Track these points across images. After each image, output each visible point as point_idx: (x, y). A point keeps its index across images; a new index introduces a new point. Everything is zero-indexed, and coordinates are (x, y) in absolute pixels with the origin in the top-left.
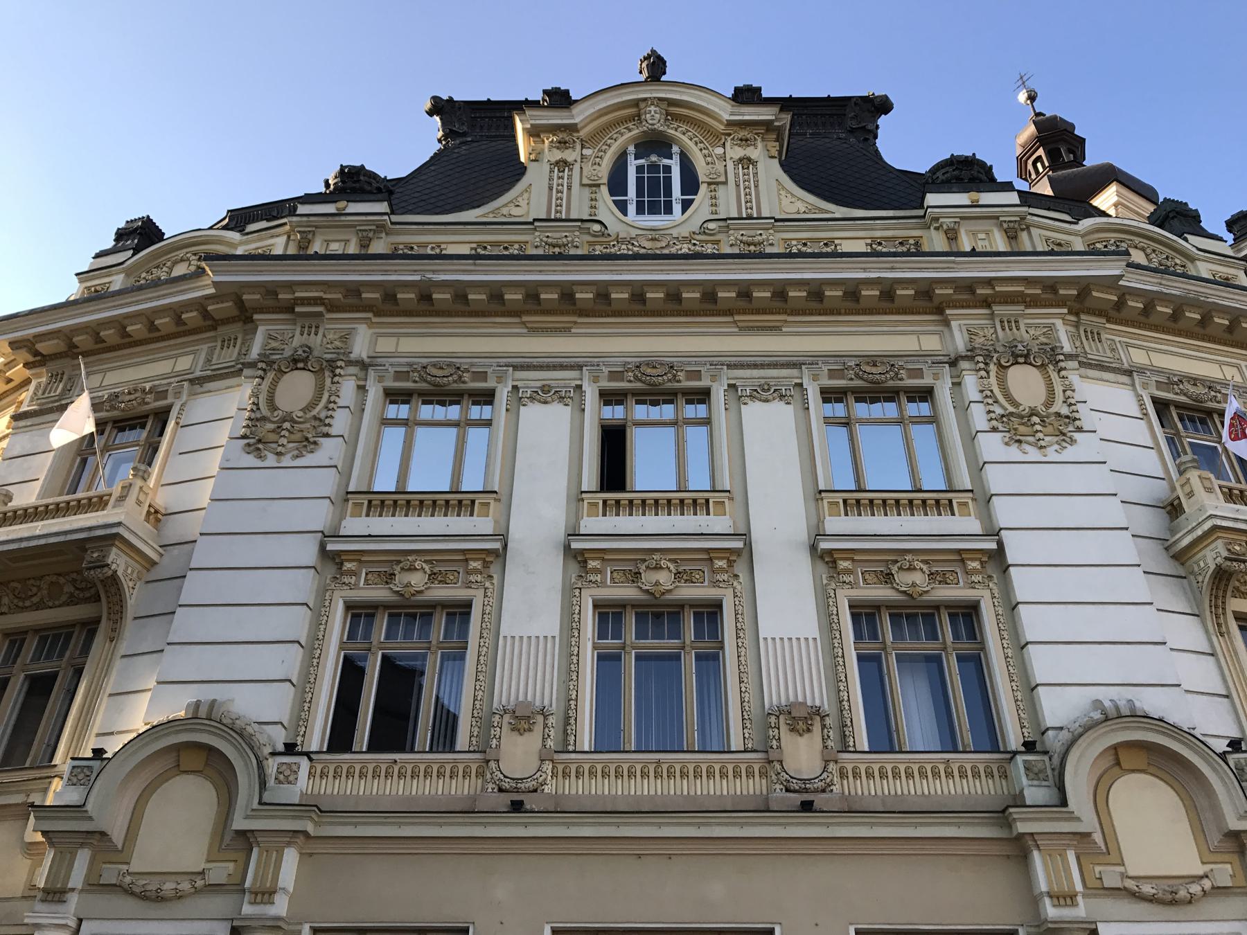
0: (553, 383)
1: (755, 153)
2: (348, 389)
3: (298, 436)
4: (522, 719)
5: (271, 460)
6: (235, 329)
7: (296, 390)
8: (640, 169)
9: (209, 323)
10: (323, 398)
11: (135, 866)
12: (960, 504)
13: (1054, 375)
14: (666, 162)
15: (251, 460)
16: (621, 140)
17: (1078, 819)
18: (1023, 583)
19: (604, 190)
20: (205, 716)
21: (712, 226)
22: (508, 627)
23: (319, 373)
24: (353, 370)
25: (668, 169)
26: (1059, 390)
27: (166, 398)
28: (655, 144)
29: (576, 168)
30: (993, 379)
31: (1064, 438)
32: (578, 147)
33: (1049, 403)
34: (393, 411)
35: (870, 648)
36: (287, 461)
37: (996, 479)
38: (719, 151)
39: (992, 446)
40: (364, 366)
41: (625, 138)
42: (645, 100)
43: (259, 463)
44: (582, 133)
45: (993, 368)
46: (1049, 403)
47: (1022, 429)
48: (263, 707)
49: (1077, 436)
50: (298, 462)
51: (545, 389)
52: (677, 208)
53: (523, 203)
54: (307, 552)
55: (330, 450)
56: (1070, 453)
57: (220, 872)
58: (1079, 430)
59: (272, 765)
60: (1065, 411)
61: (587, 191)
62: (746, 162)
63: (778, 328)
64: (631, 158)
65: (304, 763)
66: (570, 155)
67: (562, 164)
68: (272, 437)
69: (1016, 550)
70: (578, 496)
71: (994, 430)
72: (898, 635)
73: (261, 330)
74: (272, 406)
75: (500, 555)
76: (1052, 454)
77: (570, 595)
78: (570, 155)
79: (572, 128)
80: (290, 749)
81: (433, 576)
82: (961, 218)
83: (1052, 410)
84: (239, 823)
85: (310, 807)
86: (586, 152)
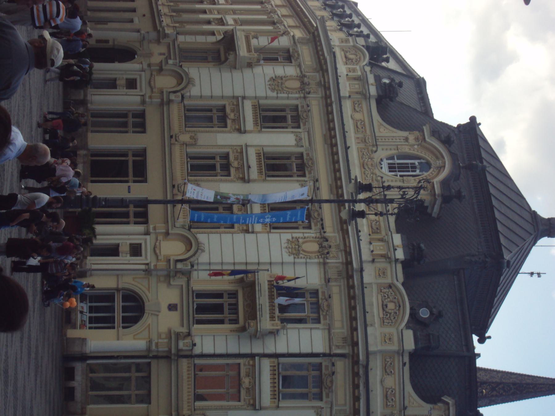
2: (297, 95)
5: (267, 83)
8: (414, 164)
11: (156, 77)
15: (267, 78)
16: (427, 157)
18: (239, 237)
19: (396, 151)
20: (190, 82)
23: (300, 88)
25: (415, 171)
28: (426, 166)
30: (312, 239)
31: (291, 254)
32: (417, 143)
41: (429, 157)
44: (423, 144)
48: (194, 91)
49: (292, 257)
50: (268, 89)
52: (393, 173)
54: (238, 92)
55: (274, 94)
58: (295, 258)
61: (395, 147)
64: (419, 161)
65: (180, 99)
67: (407, 139)
69: (250, 237)
70: (263, 146)
71: (293, 238)
73: (317, 74)
74: (286, 81)
75: (239, 131)
76: (284, 250)
77: (231, 146)
79: (424, 139)
80: (183, 97)
83: (301, 252)
85: (170, 102)
86: (416, 147)
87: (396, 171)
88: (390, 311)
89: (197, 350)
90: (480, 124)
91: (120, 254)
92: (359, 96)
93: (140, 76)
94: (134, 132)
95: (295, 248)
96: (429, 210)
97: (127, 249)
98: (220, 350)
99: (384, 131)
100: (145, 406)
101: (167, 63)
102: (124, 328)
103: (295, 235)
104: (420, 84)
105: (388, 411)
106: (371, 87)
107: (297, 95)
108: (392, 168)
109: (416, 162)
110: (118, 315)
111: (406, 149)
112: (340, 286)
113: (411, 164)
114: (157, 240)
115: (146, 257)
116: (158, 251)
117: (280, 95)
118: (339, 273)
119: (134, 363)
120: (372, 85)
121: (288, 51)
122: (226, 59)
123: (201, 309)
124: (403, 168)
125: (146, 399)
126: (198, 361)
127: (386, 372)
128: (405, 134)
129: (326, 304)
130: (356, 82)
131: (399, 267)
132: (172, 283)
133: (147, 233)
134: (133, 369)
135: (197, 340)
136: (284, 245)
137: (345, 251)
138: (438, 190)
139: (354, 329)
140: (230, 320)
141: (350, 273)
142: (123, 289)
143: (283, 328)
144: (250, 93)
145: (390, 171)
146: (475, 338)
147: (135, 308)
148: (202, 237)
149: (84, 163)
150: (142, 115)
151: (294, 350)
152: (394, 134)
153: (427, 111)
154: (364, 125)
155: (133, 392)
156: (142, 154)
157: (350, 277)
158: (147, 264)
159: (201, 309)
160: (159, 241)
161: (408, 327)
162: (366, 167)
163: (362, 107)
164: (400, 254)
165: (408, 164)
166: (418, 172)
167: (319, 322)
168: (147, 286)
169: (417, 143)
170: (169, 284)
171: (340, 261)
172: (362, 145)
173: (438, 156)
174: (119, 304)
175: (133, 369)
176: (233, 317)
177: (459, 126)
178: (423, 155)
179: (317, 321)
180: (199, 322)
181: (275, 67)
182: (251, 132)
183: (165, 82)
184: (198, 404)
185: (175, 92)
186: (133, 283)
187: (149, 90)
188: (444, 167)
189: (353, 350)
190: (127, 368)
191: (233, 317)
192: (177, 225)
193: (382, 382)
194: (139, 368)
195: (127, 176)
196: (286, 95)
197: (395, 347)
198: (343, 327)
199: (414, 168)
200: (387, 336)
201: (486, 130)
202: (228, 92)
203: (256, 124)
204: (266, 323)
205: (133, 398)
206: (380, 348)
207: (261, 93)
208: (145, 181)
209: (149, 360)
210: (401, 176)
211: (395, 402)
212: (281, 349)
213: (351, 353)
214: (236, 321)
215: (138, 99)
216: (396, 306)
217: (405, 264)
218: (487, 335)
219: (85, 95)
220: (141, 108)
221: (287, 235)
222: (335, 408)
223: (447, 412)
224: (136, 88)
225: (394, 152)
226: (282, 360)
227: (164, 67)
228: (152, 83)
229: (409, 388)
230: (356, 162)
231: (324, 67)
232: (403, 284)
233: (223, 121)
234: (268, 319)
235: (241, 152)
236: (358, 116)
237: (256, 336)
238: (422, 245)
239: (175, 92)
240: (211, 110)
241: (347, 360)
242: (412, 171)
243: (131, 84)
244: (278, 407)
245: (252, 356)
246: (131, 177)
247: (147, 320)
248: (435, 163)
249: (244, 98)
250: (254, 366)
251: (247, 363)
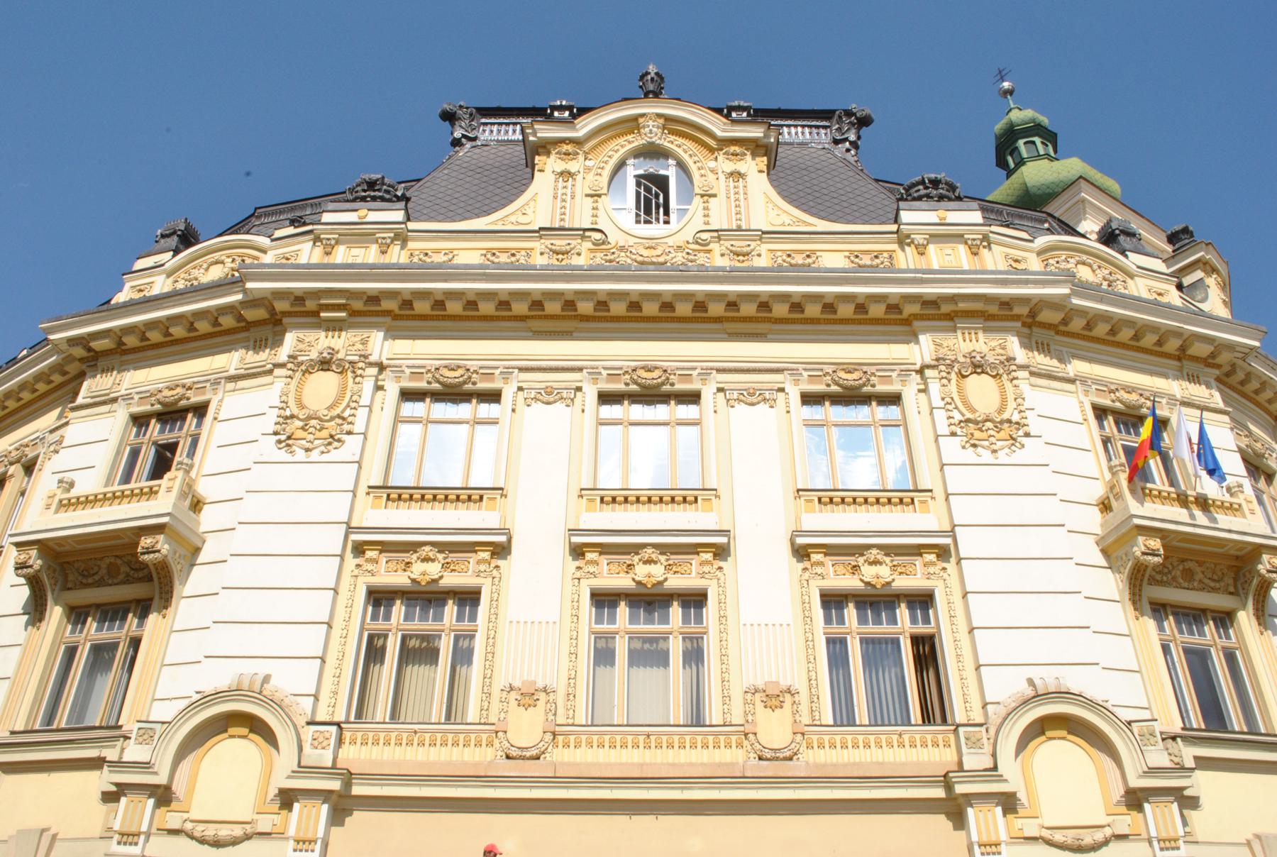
0: (555, 385)
1: (742, 166)
3: (325, 433)
6: (267, 331)
7: (321, 389)
9: (243, 324)
11: (194, 815)
12: (921, 502)
13: (1008, 385)
15: (283, 455)
16: (622, 151)
17: (1006, 781)
21: (705, 236)
24: (374, 371)
26: (1011, 397)
27: (204, 394)
29: (579, 178)
33: (1001, 410)
34: (410, 408)
35: (835, 629)
36: (315, 455)
38: (712, 164)
39: (952, 449)
40: (382, 367)
42: (643, 115)
43: (289, 458)
44: (587, 147)
45: (953, 376)
46: (1001, 410)
47: (977, 434)
49: (1024, 440)
50: (325, 457)
53: (529, 211)
54: (333, 539)
55: (352, 445)
56: (1019, 456)
58: (1027, 435)
60: (1016, 418)
62: (737, 175)
66: (573, 166)
67: (566, 175)
68: (300, 434)
69: (968, 543)
71: (953, 434)
72: (862, 620)
76: (1003, 457)
78: (573, 166)
81: (445, 566)
82: (931, 236)
83: (1006, 416)
84: (282, 780)
86: (588, 163)
103: (943, 428)
107: (368, 385)
117: (359, 426)
118: (1044, 348)
121: (140, 421)
129: (1123, 395)
136: (986, 456)
169: (581, 157)
173: (632, 124)
178: (616, 158)
188: (668, 119)
192: (976, 760)
196: (362, 414)
228: (224, 832)
248: (652, 133)
249: (350, 529)
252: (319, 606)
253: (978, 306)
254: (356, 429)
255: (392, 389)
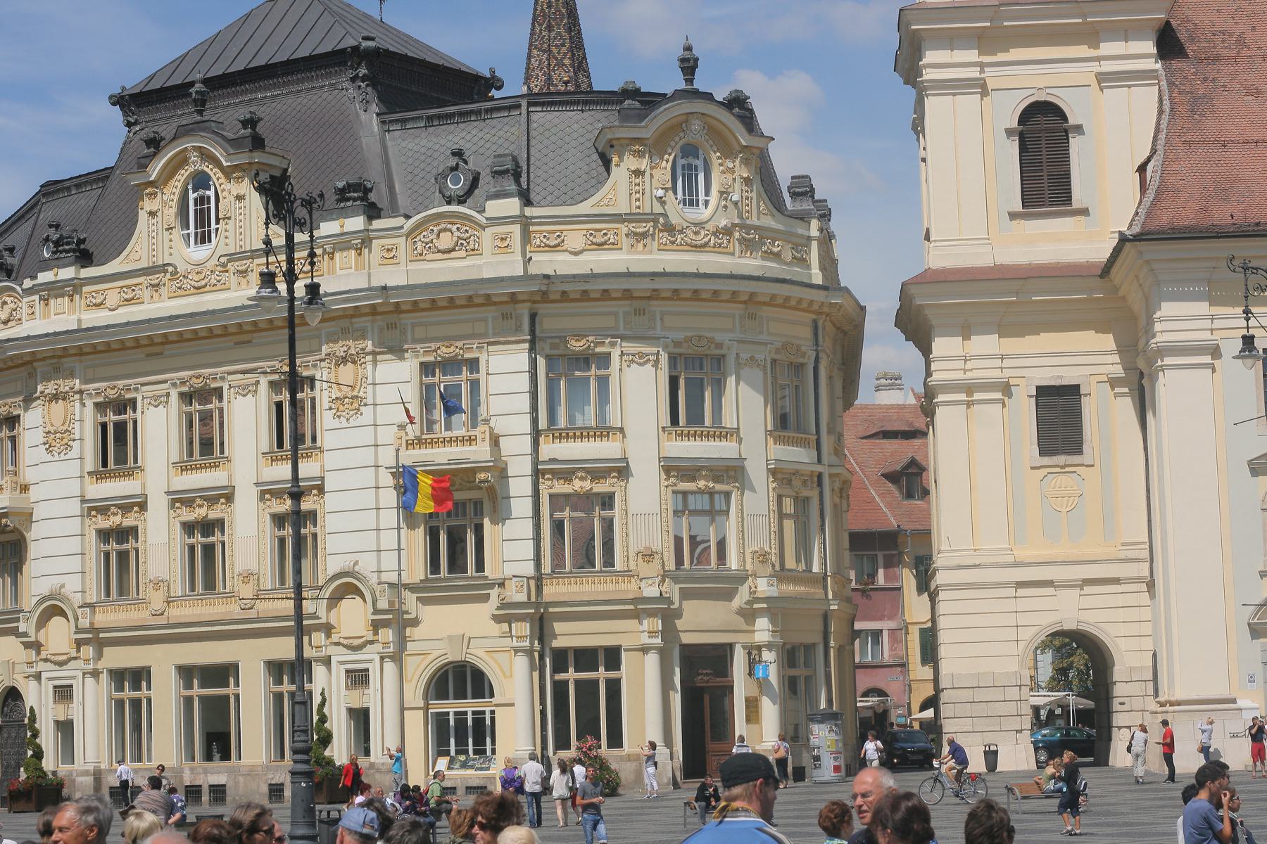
4: (157, 584)
5: (57, 457)
8: (196, 200)
10: (69, 419)
14: (208, 193)
15: (49, 457)
22: (150, 541)
24: (77, 396)
25: (209, 198)
29: (159, 214)
37: (327, 439)
47: (341, 408)
48: (72, 586)
51: (155, 398)
52: (213, 235)
54: (75, 507)
55: (76, 445)
56: (361, 420)
57: (74, 654)
58: (365, 405)
59: (79, 612)
60: (361, 394)
61: (166, 233)
62: (240, 198)
63: (249, 342)
67: (152, 214)
71: (330, 409)
76: (352, 422)
79: (151, 184)
86: (165, 198)
87: (210, 231)
88: (455, 239)
89: (529, 569)
90: (124, 88)
91: (365, 705)
92: (77, 297)
93: (50, 679)
94: (149, 688)
95: (351, 402)
96: (277, 173)
97: (355, 693)
98: (527, 528)
99: (138, 252)
100: (623, 653)
101: (25, 635)
102: (492, 695)
103: (326, 405)
104: (51, 190)
105: (626, 242)
106: (59, 278)
107: (77, 404)
108: (204, 238)
109: (192, 196)
110: (470, 706)
111: (170, 213)
112: (414, 325)
113: (196, 205)
114: (337, 644)
115: (370, 661)
116: (359, 641)
119: (552, 676)
120: (56, 275)
122: (15, 530)
123: (457, 564)
124: (203, 218)
125: (613, 657)
126: (547, 568)
127: (558, 245)
128: (143, 216)
130: (52, 302)
131: (377, 224)
132: (413, 616)
133: (327, 662)
134: (561, 676)
135: (509, 570)
137: (352, 316)
138: (242, 159)
139: (488, 300)
140: (476, 514)
141: (391, 309)
142: (426, 698)
143: (486, 421)
144: (74, 488)
145: (210, 241)
146: (494, 93)
147: (461, 679)
148: (332, 565)
149: (206, 772)
150: (118, 676)
151: (524, 402)
152: (144, 234)
153: (101, 177)
154: (128, 287)
155: (602, 674)
156: (187, 673)
157: (397, 308)
158: (382, 658)
159: (457, 564)
160: (342, 640)
161: (482, 211)
162: (203, 283)
163: (97, 292)
164: (356, 223)
165: (196, 211)
166: (211, 193)
167: (477, 360)
168: (421, 657)
169: (159, 195)
170: (415, 622)
171: (369, 324)
172: (164, 290)
174: (451, 707)
175: (561, 676)
176: (470, 509)
177: (129, 125)
179: (473, 364)
180: (480, 566)
181: (27, 445)
182: (144, 486)
183: (58, 635)
184: (619, 565)
185: (77, 619)
186: (414, 682)
187: (72, 664)
189: (524, 301)
190: (560, 690)
191: (470, 509)
193: (576, 254)
194: (559, 666)
195: (227, 697)
197: (516, 229)
198: (485, 320)
199: (202, 200)
200: (499, 243)
201: (132, 80)
202: (74, 525)
203: (129, 474)
204: (479, 452)
205: (612, 674)
206: (518, 257)
207: (74, 468)
208: (235, 666)
209: (547, 651)
210: (217, 222)
211: (609, 230)
212: (525, 424)
213: (528, 304)
214: (478, 505)
215: (90, 681)
216: (445, 230)
217: (373, 212)
218: (488, 76)
219: (86, 773)
220: (104, 677)
221: (326, 419)
222: (621, 332)
223: (623, 142)
224: (71, 686)
225: (177, 233)
226: (543, 424)
227: (33, 639)
229: (585, 208)
230: (192, 299)
231: (28, 358)
232: (408, 217)
233: (125, 534)
234: (473, 448)
235: (180, 500)
236: (113, 298)
237: (502, 473)
238: (340, 185)
239: (77, 619)
240: (107, 555)
241: (540, 312)
242: (209, 203)
243: (64, 693)
244: (621, 430)
245: (537, 474)
246: (230, 690)
247: (479, 656)
248: (196, 164)
250: (552, 471)
251: (549, 483)
252: (74, 545)
253: (341, 313)
254: (77, 436)
255: (89, 403)
